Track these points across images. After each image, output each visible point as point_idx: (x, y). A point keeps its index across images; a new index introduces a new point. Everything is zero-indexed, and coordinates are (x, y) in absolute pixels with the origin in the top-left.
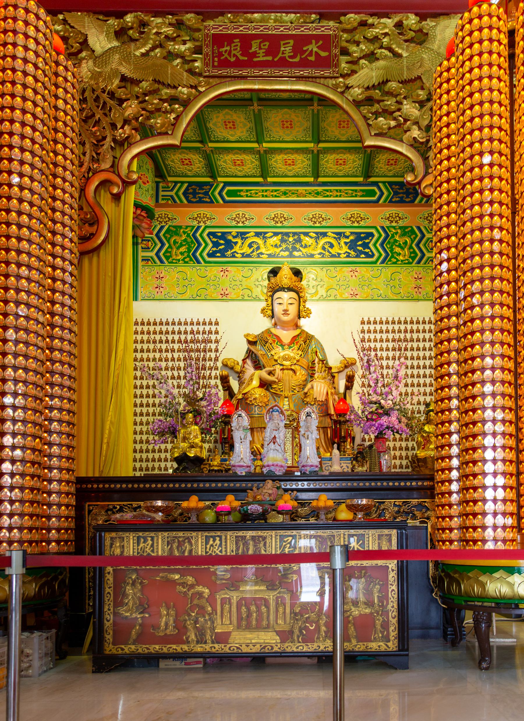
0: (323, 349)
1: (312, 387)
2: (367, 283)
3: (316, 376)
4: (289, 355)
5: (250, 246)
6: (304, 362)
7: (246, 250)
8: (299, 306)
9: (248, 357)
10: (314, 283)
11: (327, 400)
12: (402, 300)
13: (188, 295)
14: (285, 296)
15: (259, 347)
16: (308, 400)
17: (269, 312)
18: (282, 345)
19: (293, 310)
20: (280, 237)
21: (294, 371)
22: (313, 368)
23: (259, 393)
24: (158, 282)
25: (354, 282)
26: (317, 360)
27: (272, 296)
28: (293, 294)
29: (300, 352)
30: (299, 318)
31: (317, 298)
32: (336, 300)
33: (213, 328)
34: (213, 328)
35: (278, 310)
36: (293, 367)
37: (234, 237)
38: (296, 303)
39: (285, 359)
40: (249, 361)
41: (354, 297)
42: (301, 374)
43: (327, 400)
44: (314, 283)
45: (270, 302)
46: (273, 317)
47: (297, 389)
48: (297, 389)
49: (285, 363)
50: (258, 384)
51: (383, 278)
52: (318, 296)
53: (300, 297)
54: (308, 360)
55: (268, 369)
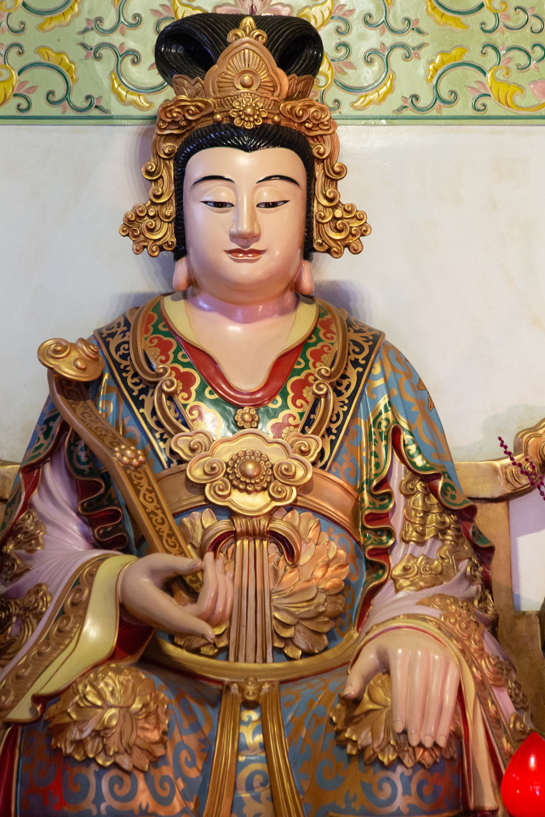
0: (427, 407)
1: (384, 668)
3: (397, 560)
4: (258, 458)
6: (334, 493)
8: (310, 197)
9: (51, 455)
10: (374, 39)
11: (459, 737)
14: (245, 173)
15: (107, 406)
16: (364, 737)
17: (164, 232)
18: (229, 403)
19: (279, 231)
21: (288, 548)
22: (379, 519)
23: (116, 698)
26: (398, 475)
27: (181, 161)
28: (281, 160)
29: (314, 443)
30: (308, 250)
31: (388, 109)
32: (480, 115)
35: (209, 229)
36: (280, 525)
38: (295, 195)
39: (238, 476)
40: (54, 479)
42: (323, 559)
43: (459, 737)
44: (374, 39)
45: (167, 187)
46: (180, 250)
47: (302, 642)
48: (302, 642)
49: (241, 500)
50: (111, 640)
52: (394, 102)
53: (309, 162)
54: (356, 473)
55: (163, 560)
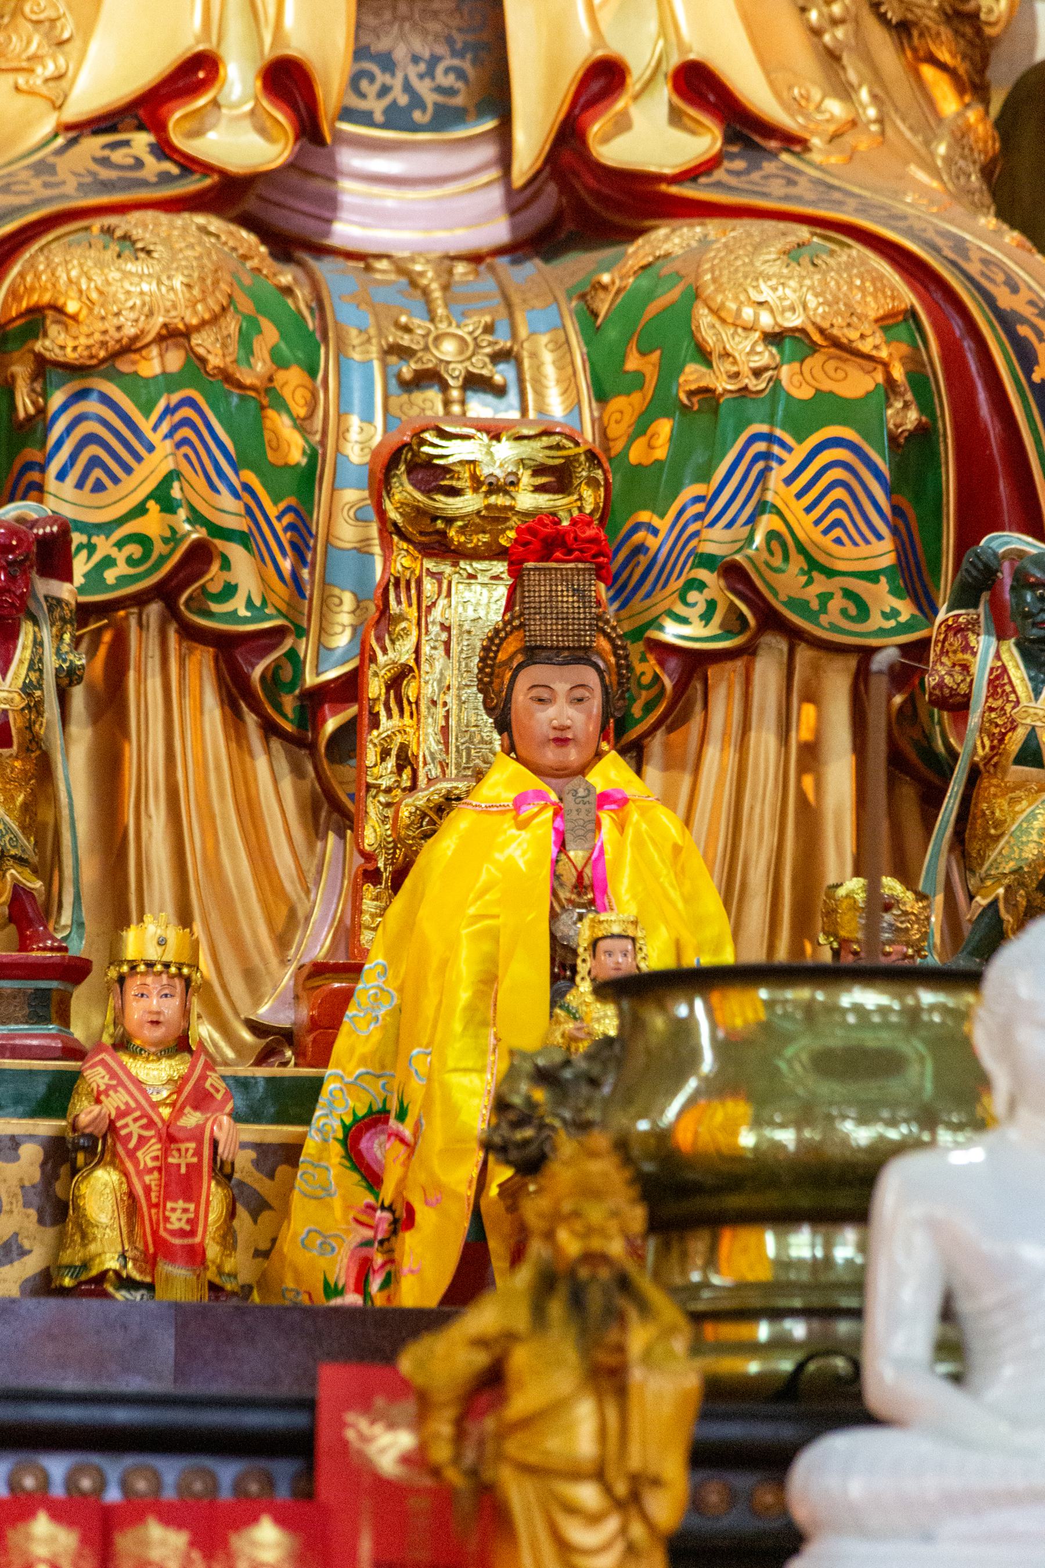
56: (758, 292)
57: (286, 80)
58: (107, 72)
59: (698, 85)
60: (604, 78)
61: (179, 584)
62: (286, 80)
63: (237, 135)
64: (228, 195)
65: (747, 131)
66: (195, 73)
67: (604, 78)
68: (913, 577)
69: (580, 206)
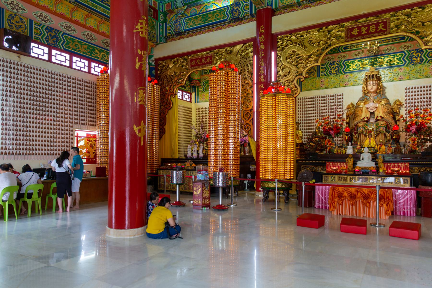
2: (407, 73)
5: (356, 65)
7: (354, 67)
12: (425, 77)
13: (332, 86)
20: (368, 61)
24: (322, 83)
25: (401, 74)
33: (341, 97)
34: (341, 97)
37: (350, 63)
41: (401, 79)
51: (415, 70)
56: (381, 123)
57: (367, 118)
58: (362, 118)
59: (381, 116)
60: (377, 117)
61: (362, 132)
62: (367, 118)
63: (366, 119)
64: (366, 121)
65: (382, 118)
66: (364, 118)
67: (377, 117)
68: (386, 131)
69: (377, 120)
